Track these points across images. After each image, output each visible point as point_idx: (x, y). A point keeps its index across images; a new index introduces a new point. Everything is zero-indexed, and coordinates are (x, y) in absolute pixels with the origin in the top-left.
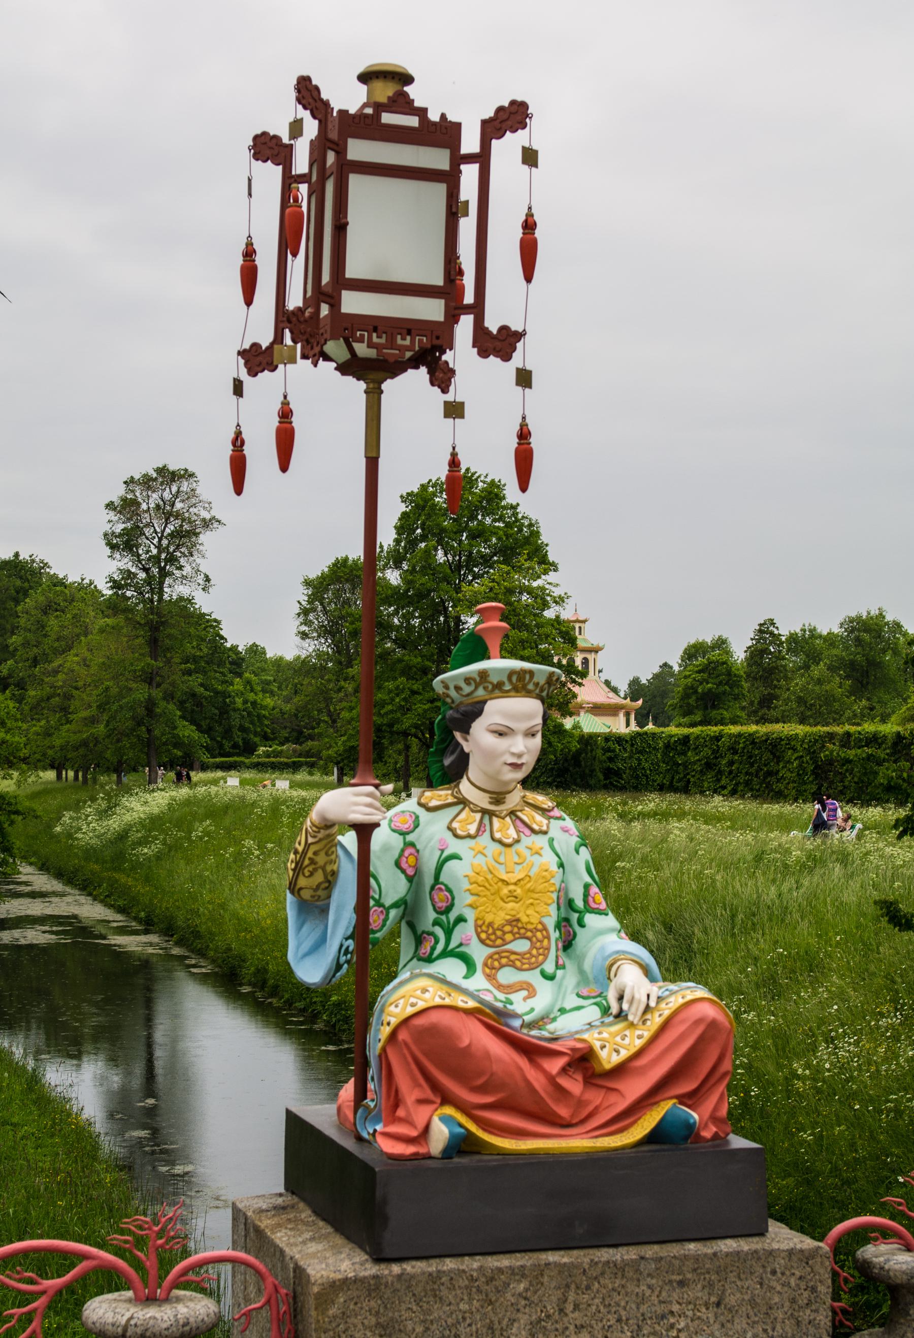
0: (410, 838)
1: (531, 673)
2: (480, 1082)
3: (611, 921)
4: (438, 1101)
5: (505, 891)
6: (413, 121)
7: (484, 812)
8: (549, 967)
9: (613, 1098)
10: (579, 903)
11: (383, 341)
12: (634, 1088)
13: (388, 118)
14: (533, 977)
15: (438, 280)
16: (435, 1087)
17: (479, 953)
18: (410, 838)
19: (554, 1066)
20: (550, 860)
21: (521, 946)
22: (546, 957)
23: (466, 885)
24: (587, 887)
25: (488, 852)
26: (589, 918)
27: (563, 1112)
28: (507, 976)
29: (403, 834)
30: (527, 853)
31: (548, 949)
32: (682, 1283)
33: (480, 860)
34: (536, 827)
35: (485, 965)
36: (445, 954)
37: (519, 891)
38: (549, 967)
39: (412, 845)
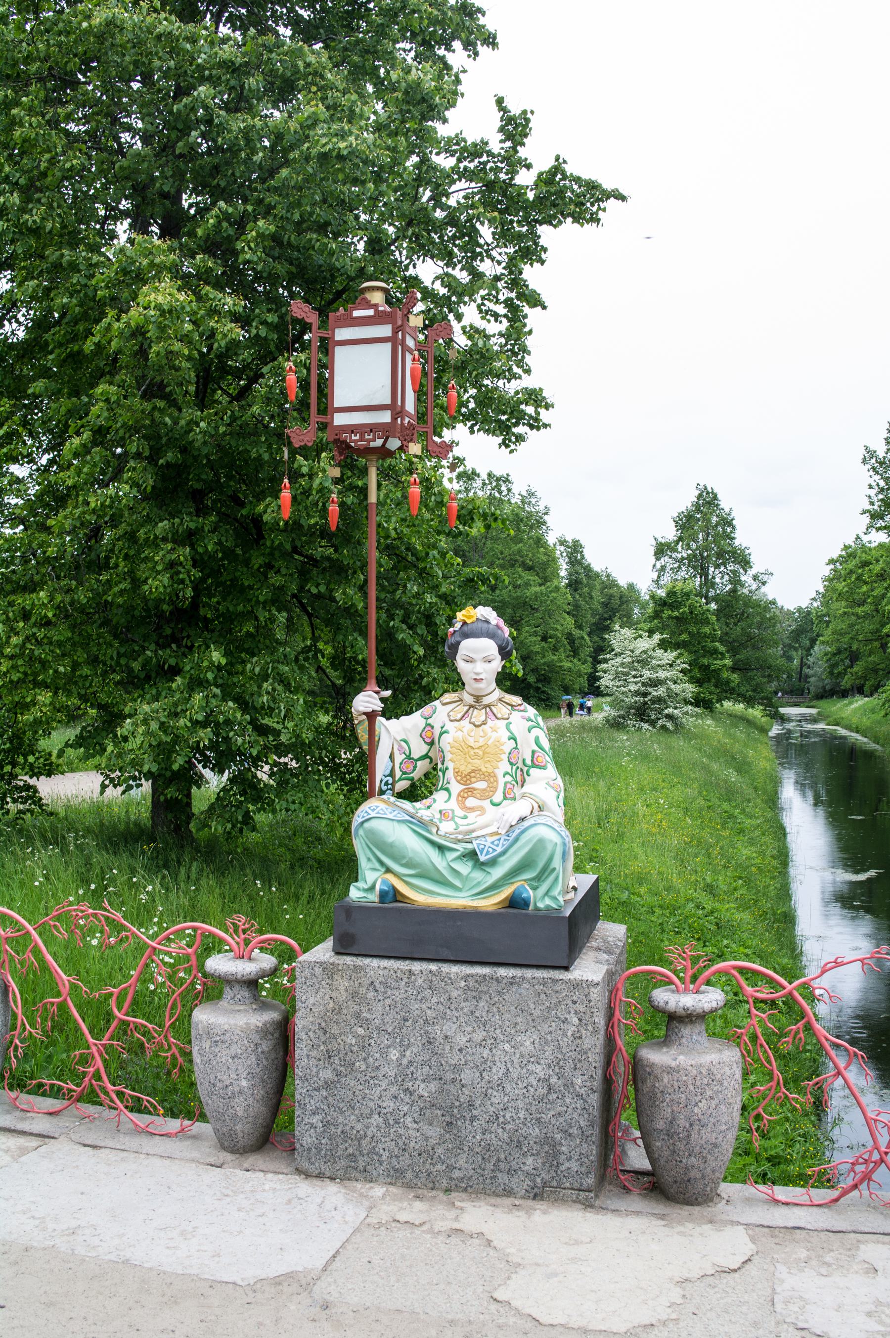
0: (429, 721)
2: (404, 861)
3: (551, 771)
4: (383, 870)
5: (472, 752)
6: (371, 312)
7: (471, 706)
8: (498, 797)
9: (489, 876)
10: (529, 762)
11: (357, 438)
12: (497, 873)
13: (356, 313)
14: (486, 804)
15: (388, 402)
16: (382, 863)
17: (456, 788)
18: (429, 721)
19: (451, 856)
20: (504, 735)
21: (481, 785)
22: (494, 792)
23: (449, 748)
24: (533, 752)
25: (465, 730)
26: (533, 771)
27: (458, 883)
28: (471, 802)
29: (426, 719)
30: (489, 730)
31: (496, 788)
33: (460, 734)
34: (499, 716)
35: (459, 795)
36: (442, 789)
37: (481, 753)
38: (498, 797)
39: (429, 725)
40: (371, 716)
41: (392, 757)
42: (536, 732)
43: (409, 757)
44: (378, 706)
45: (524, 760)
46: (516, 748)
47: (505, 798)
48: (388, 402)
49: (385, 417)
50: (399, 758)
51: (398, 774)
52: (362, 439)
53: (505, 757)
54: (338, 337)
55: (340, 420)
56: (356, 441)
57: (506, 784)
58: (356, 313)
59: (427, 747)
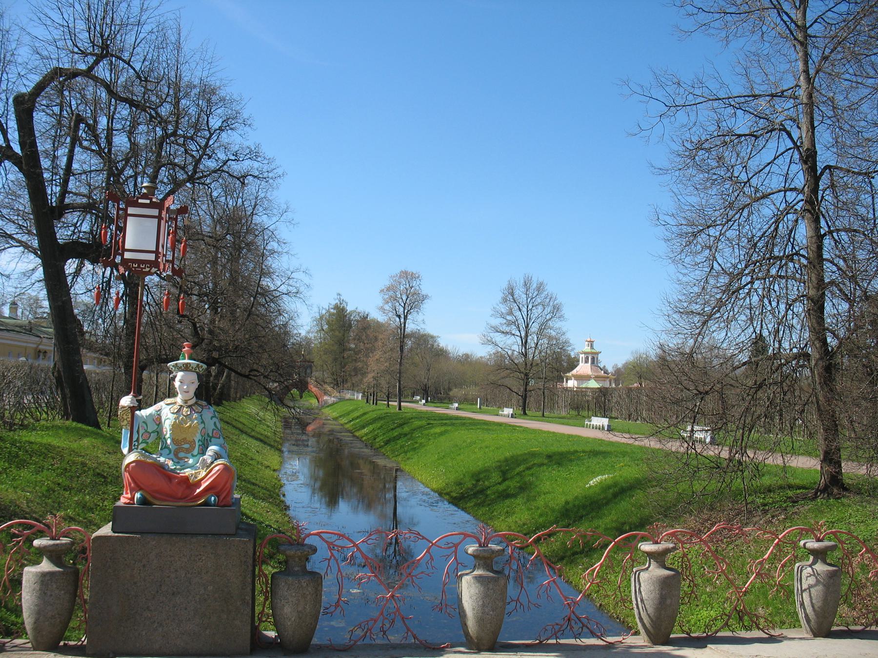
1: (190, 364)
6: (148, 201)
8: (195, 452)
15: (154, 249)
24: (213, 430)
32: (204, 546)
38: (195, 452)
40: (133, 409)
41: (138, 432)
42: (214, 419)
43: (146, 431)
44: (136, 404)
45: (208, 434)
46: (204, 428)
47: (199, 453)
48: (154, 249)
49: (152, 257)
50: (141, 432)
51: (141, 440)
52: (139, 267)
53: (199, 432)
54: (129, 212)
55: (127, 255)
56: (135, 268)
57: (199, 445)
58: (140, 201)
59: (157, 427)
